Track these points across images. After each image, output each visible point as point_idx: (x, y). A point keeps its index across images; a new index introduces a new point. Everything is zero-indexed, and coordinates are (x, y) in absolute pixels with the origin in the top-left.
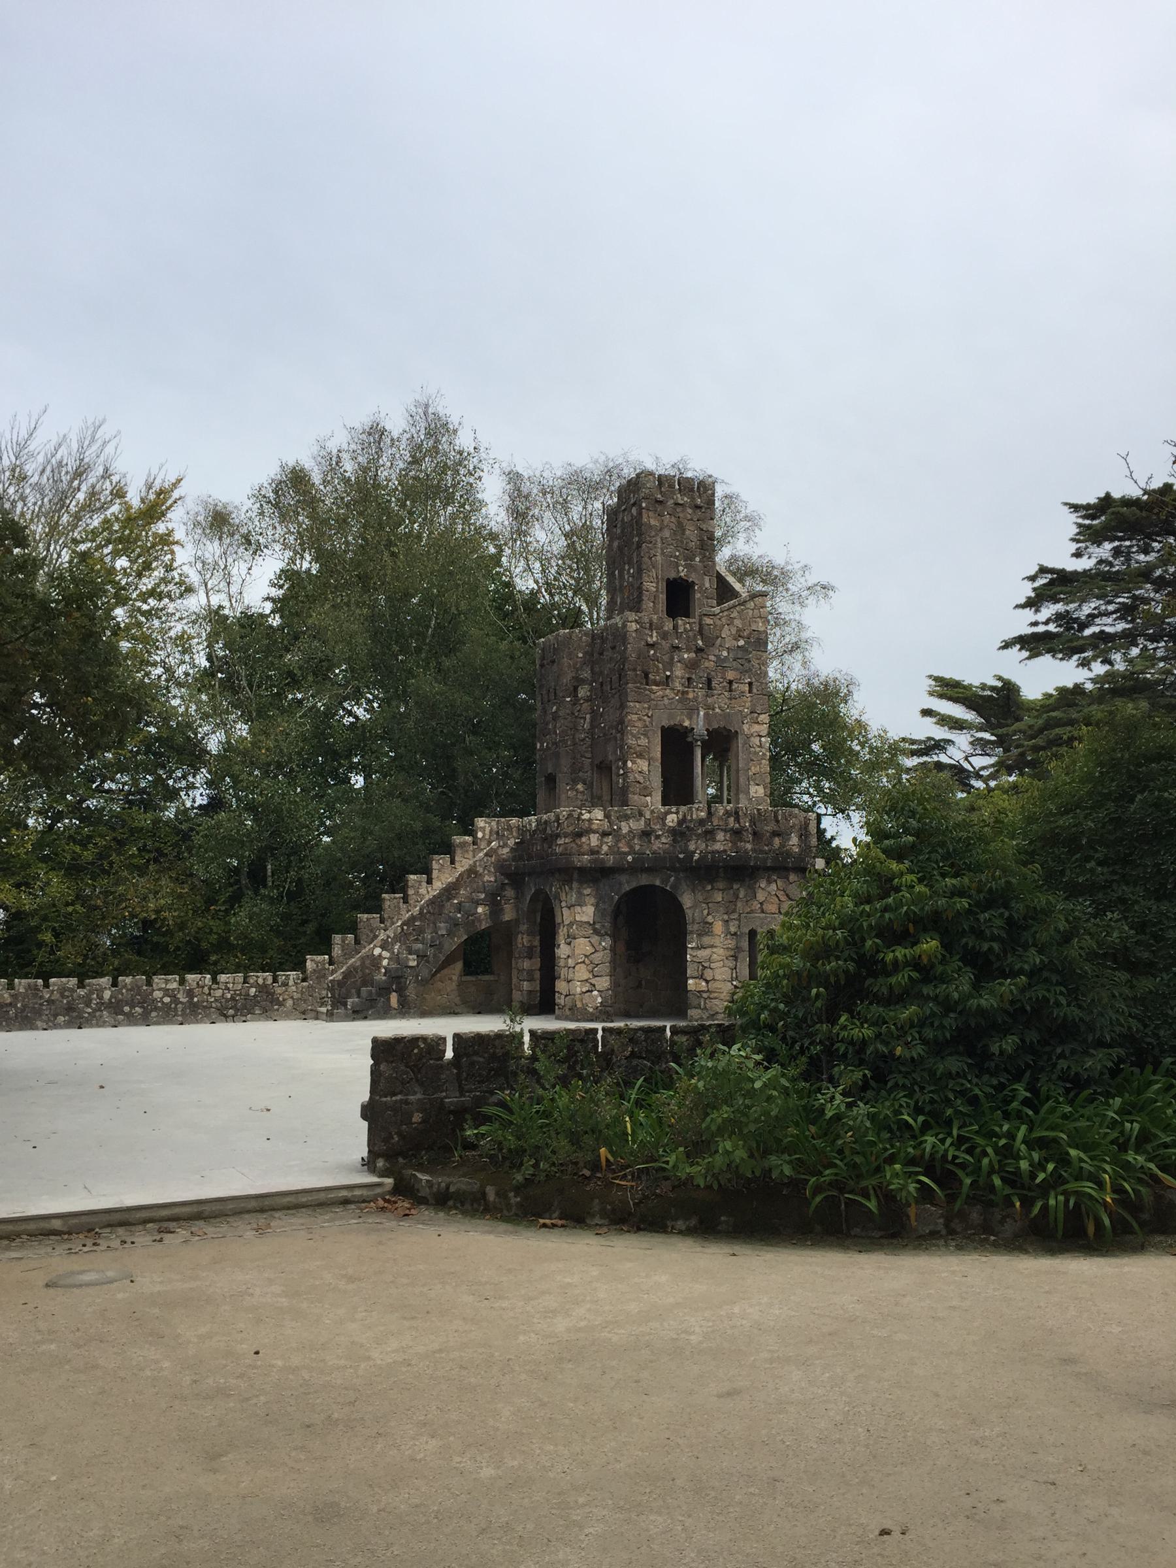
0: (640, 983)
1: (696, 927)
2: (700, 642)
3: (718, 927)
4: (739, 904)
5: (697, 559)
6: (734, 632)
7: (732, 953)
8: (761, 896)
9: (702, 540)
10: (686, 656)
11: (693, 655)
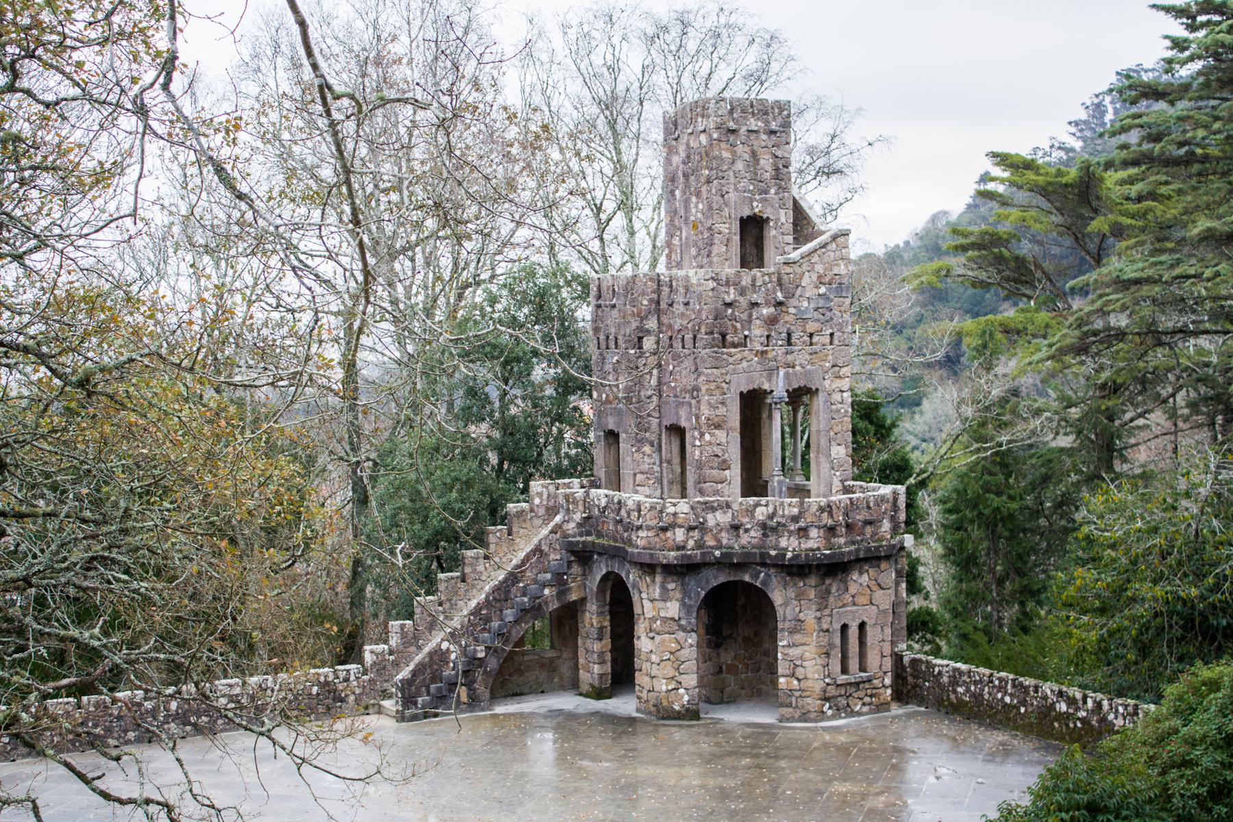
0: (721, 668)
1: (787, 625)
2: (779, 294)
4: (831, 599)
5: (773, 191)
6: (815, 279)
8: (853, 589)
9: (777, 169)
10: (765, 311)
11: (772, 310)
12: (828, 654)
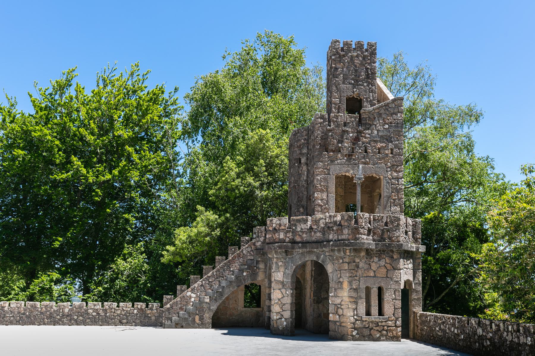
3: (346, 285)
7: (354, 300)
12: (356, 303)
